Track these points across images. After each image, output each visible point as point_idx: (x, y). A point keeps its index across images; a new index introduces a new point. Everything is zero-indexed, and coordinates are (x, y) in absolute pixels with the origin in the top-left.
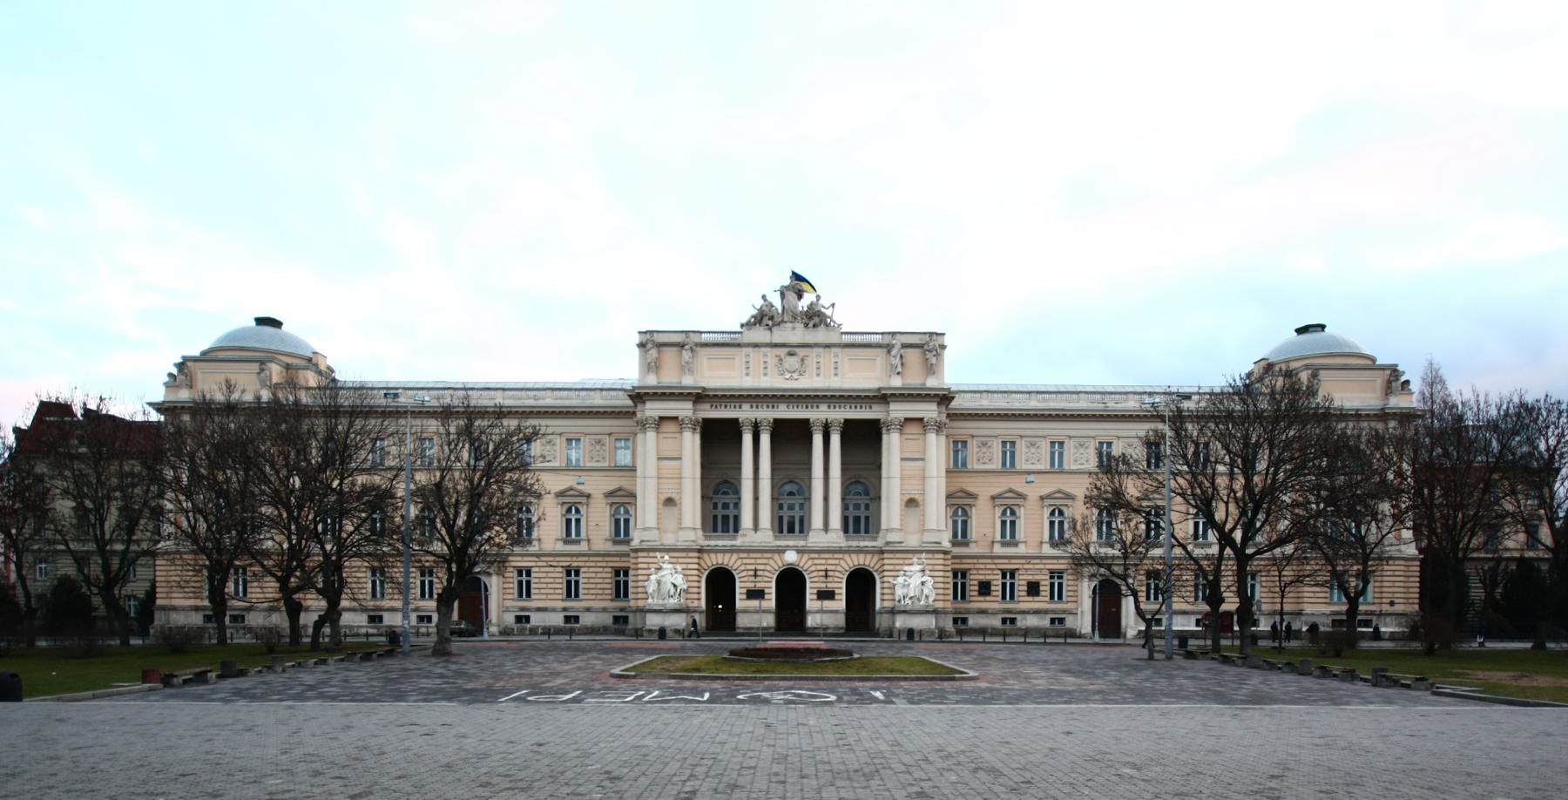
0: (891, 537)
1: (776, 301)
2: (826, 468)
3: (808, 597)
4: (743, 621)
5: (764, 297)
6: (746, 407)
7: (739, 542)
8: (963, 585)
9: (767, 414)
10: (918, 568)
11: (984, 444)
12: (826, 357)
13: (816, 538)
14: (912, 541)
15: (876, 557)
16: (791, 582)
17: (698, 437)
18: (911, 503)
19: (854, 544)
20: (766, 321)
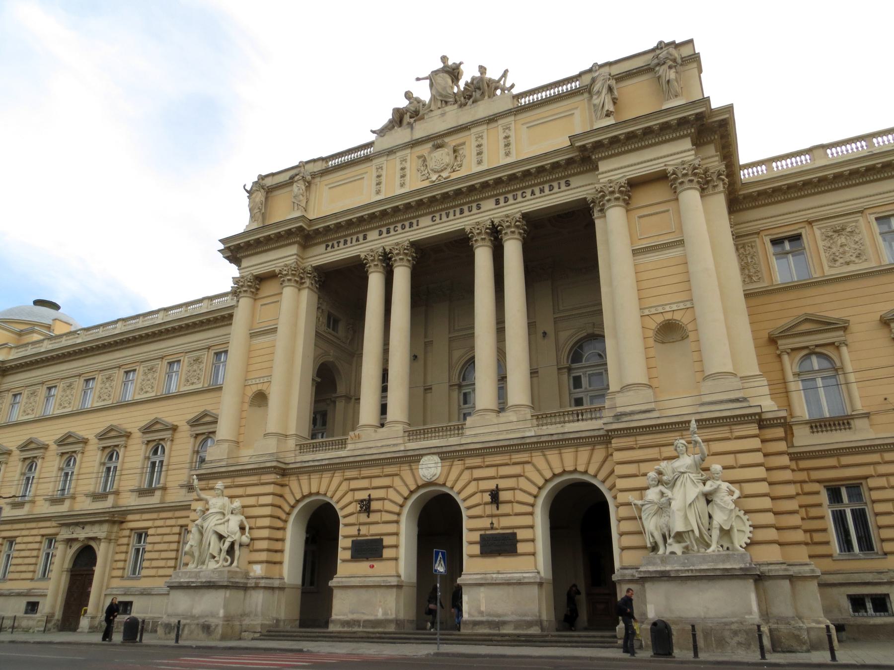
0: (624, 402)
1: (424, 93)
2: (501, 303)
3: (467, 549)
4: (474, 605)
5: (408, 95)
6: (373, 235)
7: (352, 449)
8: (860, 517)
9: (400, 238)
10: (686, 461)
11: (839, 231)
12: (493, 137)
13: (481, 428)
14: (679, 404)
15: (600, 453)
16: (438, 521)
17: (305, 293)
18: (670, 331)
19: (553, 429)
20: (407, 119)
